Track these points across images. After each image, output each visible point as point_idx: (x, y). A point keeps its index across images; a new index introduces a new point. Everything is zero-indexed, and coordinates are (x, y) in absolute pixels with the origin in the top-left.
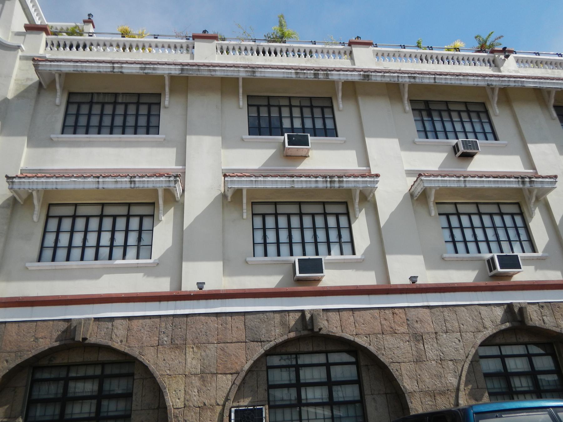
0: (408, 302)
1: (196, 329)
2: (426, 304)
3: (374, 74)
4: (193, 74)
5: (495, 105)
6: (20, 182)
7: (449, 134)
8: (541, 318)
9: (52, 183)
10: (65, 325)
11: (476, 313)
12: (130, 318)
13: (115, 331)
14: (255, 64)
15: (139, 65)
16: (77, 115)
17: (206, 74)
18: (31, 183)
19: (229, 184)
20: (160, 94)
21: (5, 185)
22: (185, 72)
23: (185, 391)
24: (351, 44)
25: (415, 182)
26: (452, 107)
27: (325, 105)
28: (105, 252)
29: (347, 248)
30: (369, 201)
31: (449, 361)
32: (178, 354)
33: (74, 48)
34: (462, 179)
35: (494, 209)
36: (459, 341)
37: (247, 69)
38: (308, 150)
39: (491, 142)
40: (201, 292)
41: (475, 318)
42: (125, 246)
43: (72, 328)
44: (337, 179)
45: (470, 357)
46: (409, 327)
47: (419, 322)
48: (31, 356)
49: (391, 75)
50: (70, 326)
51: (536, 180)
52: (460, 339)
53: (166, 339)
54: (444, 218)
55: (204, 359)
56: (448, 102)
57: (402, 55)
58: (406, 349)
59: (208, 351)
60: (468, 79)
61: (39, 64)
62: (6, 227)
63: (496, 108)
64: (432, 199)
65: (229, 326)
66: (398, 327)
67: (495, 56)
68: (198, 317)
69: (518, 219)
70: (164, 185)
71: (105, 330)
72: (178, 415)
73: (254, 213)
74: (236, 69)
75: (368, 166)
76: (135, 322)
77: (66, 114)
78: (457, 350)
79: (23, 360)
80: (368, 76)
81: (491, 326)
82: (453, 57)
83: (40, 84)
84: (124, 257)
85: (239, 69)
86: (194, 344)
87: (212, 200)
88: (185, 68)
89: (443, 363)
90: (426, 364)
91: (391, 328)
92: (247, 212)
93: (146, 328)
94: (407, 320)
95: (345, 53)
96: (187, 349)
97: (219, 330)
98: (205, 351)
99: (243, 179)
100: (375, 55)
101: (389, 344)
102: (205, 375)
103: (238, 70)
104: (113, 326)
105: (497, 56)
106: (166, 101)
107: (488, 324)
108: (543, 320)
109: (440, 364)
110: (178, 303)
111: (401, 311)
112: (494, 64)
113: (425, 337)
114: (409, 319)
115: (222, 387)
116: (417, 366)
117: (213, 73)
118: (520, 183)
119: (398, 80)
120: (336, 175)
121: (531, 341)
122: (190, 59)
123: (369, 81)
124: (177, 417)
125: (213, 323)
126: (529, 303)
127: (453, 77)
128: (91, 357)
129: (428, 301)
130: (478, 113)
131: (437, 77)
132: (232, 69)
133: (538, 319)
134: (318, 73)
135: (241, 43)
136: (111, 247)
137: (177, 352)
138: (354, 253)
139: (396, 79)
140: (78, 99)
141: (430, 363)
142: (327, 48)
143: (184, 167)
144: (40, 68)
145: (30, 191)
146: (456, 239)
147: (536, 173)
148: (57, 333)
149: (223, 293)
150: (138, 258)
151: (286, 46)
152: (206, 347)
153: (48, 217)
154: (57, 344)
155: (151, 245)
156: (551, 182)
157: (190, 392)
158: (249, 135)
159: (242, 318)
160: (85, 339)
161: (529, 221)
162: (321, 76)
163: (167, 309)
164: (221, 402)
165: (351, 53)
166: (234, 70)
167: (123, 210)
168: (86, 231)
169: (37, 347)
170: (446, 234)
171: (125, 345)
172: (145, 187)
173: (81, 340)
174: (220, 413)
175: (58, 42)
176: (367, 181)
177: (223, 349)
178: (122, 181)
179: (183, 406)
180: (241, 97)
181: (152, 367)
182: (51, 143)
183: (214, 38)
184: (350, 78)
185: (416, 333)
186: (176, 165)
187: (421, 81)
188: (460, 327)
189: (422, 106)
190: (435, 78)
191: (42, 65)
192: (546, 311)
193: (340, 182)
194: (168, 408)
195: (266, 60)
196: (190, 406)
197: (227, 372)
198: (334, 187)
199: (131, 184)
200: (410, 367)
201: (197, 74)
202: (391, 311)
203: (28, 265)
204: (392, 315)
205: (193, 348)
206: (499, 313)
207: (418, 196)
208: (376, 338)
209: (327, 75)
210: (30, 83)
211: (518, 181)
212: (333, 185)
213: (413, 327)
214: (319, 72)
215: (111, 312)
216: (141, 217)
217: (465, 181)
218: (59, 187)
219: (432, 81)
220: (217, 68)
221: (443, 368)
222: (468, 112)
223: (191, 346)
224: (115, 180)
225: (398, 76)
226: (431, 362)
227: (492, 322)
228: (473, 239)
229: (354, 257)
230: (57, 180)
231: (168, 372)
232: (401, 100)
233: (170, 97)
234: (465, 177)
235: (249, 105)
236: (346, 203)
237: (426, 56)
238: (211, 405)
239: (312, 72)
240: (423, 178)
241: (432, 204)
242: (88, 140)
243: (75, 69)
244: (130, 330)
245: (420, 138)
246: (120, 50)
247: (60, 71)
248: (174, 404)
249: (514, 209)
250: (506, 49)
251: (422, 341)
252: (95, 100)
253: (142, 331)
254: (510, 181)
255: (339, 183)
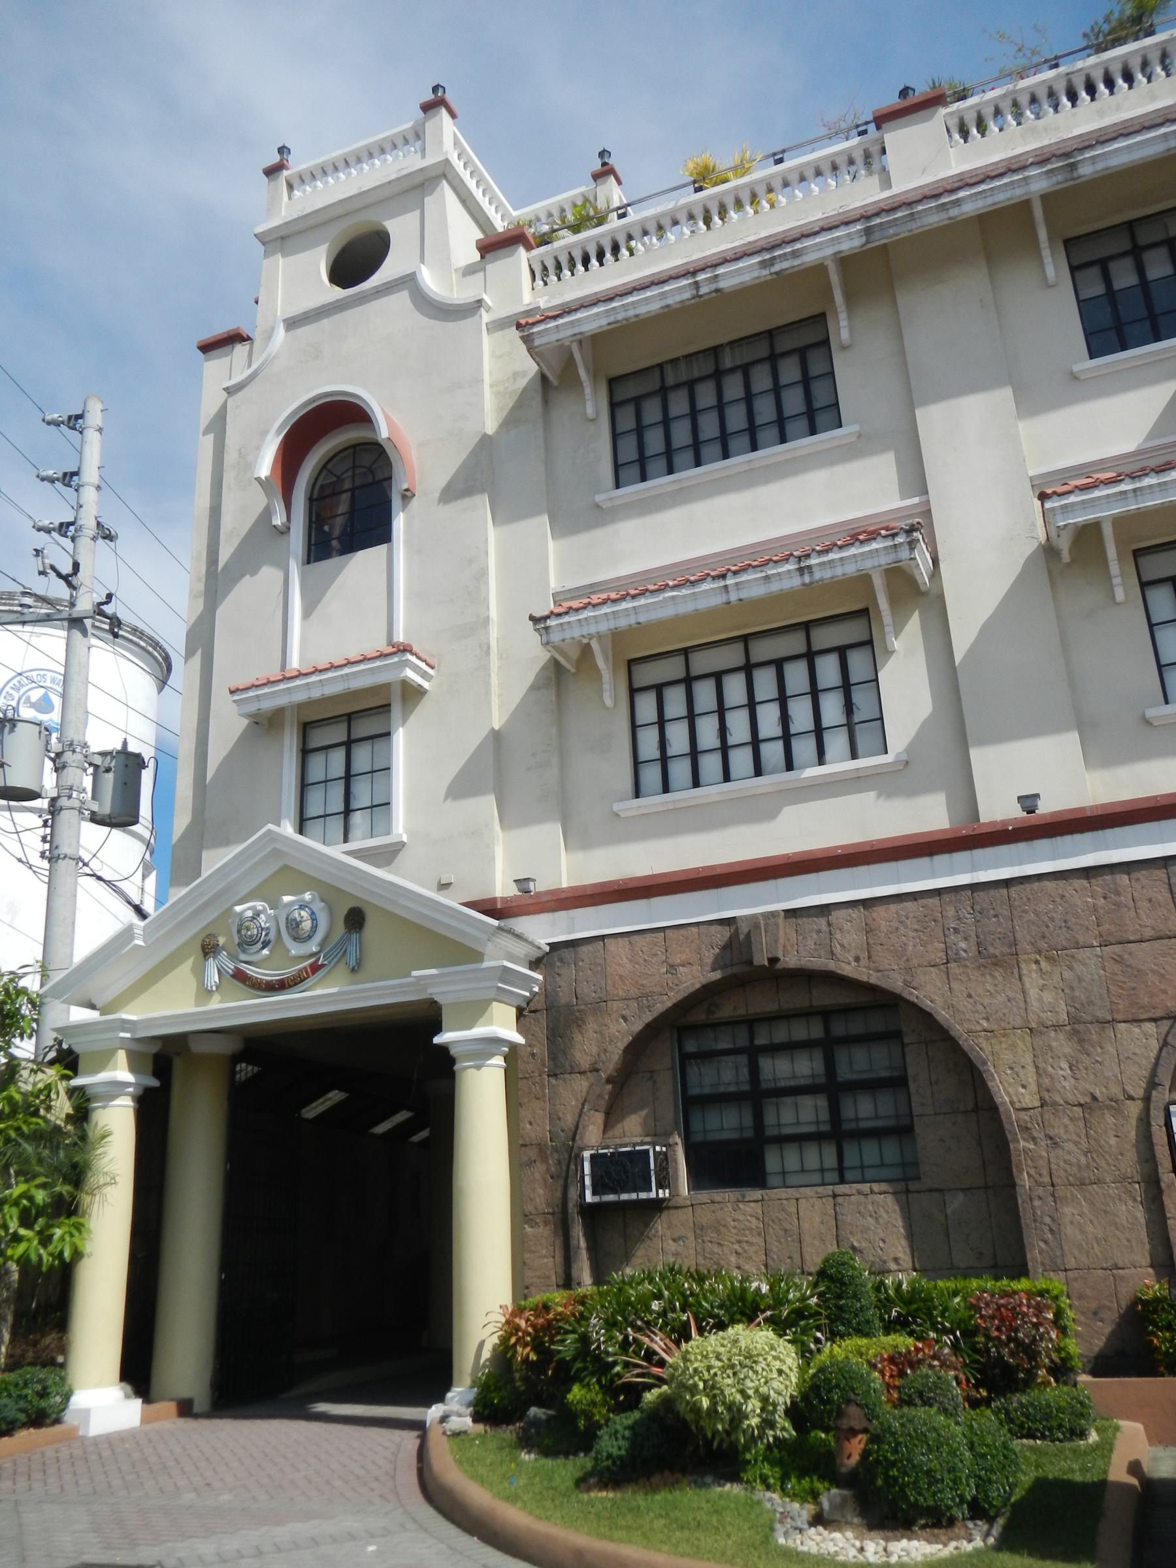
1: (1037, 914)
4: (898, 235)
6: (561, 624)
9: (628, 614)
10: (725, 933)
12: (867, 903)
13: (838, 936)
14: (1070, 136)
15: (756, 256)
16: (639, 431)
17: (934, 220)
18: (584, 623)
19: (1059, 517)
20: (823, 315)
21: (531, 638)
22: (877, 235)
23: (1037, 1067)
28: (773, 752)
32: (1000, 979)
33: (594, 262)
37: (1049, 167)
40: (1033, 819)
42: (819, 731)
43: (742, 937)
48: (669, 1004)
50: (736, 933)
53: (963, 945)
55: (1072, 989)
59: (1079, 968)
61: (532, 334)
62: (554, 731)
65: (1125, 899)
68: (1037, 884)
70: (885, 560)
71: (815, 936)
72: (1029, 1125)
73: (1144, 579)
74: (1016, 178)
76: (880, 912)
77: (615, 436)
79: (655, 1014)
83: (544, 378)
84: (821, 759)
85: (1027, 174)
86: (1039, 952)
87: (1019, 569)
88: (873, 223)
92: (1123, 584)
93: (908, 922)
96: (1023, 965)
97: (1101, 911)
98: (1071, 968)
99: (1097, 493)
102: (1081, 1027)
103: (1025, 179)
104: (829, 925)
106: (842, 329)
110: (979, 854)
115: (1135, 1054)
117: (954, 212)
122: (883, 189)
124: (1027, 1129)
125: (1079, 894)
128: (795, 999)
132: (1005, 180)
135: (1015, 86)
136: (787, 737)
137: (997, 974)
140: (631, 390)
143: (924, 498)
144: (537, 342)
145: (585, 641)
148: (712, 951)
149: (1095, 814)
150: (854, 756)
152: (1073, 957)
153: (633, 692)
154: (717, 975)
155: (881, 719)
157: (1050, 1069)
158: (1091, 358)
159: (1161, 874)
160: (774, 960)
163: (952, 873)
164: (1139, 1092)
166: (1012, 183)
167: (794, 643)
168: (721, 711)
169: (677, 985)
171: (869, 968)
172: (837, 576)
173: (766, 963)
174: (1140, 1119)
175: (556, 258)
177: (1119, 960)
178: (779, 574)
179: (1037, 1103)
180: (1046, 253)
181: (943, 1015)
182: (600, 516)
183: (935, 100)
186: (902, 499)
191: (539, 332)
194: (1001, 1109)
195: (1101, 113)
196: (1055, 1104)
197: (1142, 1017)
199: (802, 575)
201: (910, 231)
203: (617, 807)
205: (1037, 962)
210: (523, 382)
215: (820, 892)
216: (842, 652)
218: (643, 618)
220: (962, 194)
223: (1033, 956)
224: (763, 574)
230: (636, 604)
231: (985, 1024)
233: (849, 318)
235: (1073, 269)
238: (1111, 1100)
242: (676, 487)
243: (612, 319)
244: (871, 931)
246: (699, 229)
247: (581, 333)
248: (1015, 1099)
252: (670, 380)
253: (902, 930)
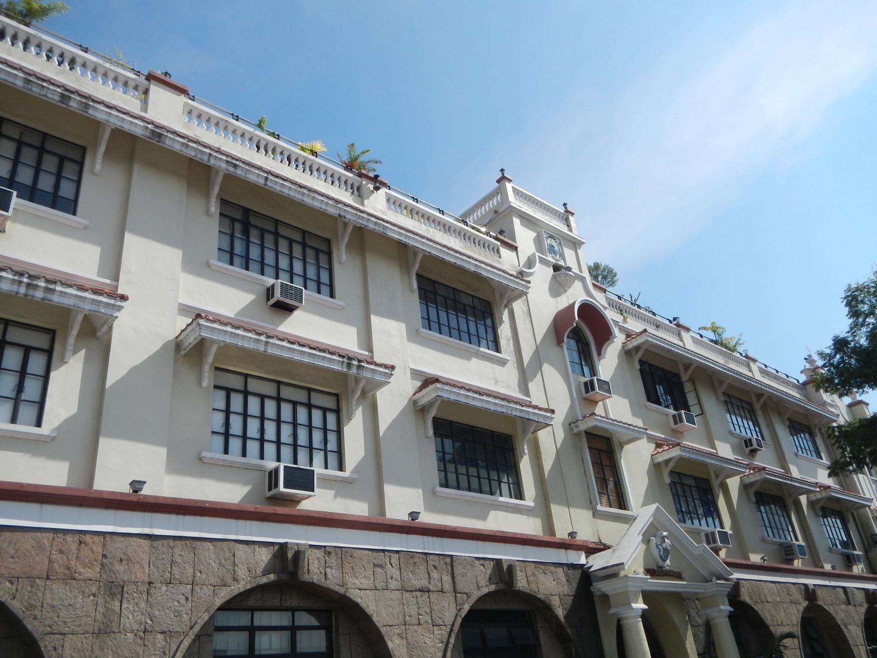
0: (115, 525)
2: (146, 531)
3: (171, 136)
5: (344, 248)
7: (266, 269)
8: (323, 571)
11: (228, 555)
24: (150, 77)
25: (188, 325)
26: (282, 231)
27: (69, 156)
29: (27, 412)
30: (98, 339)
31: (160, 633)
34: (263, 338)
35: (301, 397)
36: (187, 599)
38: (6, 218)
39: (325, 298)
41: (224, 563)
44: (42, 284)
45: (197, 629)
46: (104, 570)
47: (124, 562)
49: (200, 148)
51: (366, 366)
52: (190, 597)
54: (222, 394)
56: (279, 223)
57: (230, 129)
58: (84, 609)
60: (314, 198)
63: (344, 252)
64: (210, 359)
66: (83, 568)
67: (362, 182)
69: (331, 419)
75: (116, 279)
78: (178, 614)
80: (160, 135)
81: (245, 578)
82: (305, 161)
89: (146, 637)
90: (115, 639)
91: (68, 568)
94: (104, 556)
95: (136, 88)
100: (186, 112)
101: (53, 599)
105: (364, 182)
107: (242, 573)
108: (325, 574)
109: (141, 638)
111: (96, 538)
112: (358, 192)
113: (128, 589)
114: (108, 555)
116: (98, 641)
118: (345, 365)
119: (209, 160)
120: (44, 277)
121: (301, 605)
123: (160, 144)
126: (311, 546)
127: (293, 187)
129: (151, 527)
130: (317, 251)
131: (271, 177)
133: (318, 572)
134: (70, 97)
138: (39, 424)
139: (206, 158)
141: (123, 637)
142: (106, 68)
146: (231, 432)
147: (372, 357)
151: (26, 32)
156: (385, 373)
161: (345, 424)
162: (73, 104)
165: (146, 92)
170: (218, 420)
176: (100, 302)
184: (126, 127)
185: (114, 580)
187: (244, 175)
188: (194, 576)
189: (238, 215)
190: (266, 178)
192: (333, 561)
193: (47, 290)
198: (33, 297)
200: (82, 643)
202: (76, 538)
204: (76, 545)
206: (264, 556)
207: (188, 349)
208: (31, 586)
209: (87, 106)
211: (343, 362)
212: (31, 292)
213: (110, 570)
214: (72, 96)
217: (267, 343)
219: (262, 181)
221: (144, 645)
222: (304, 245)
225: (210, 154)
226: (125, 635)
227: (249, 571)
228: (257, 436)
229: (36, 430)
232: (207, 194)
234: (268, 337)
236: (52, 333)
237: (267, 144)
239: (59, 90)
240: (202, 322)
241: (207, 368)
245: (219, 260)
249: (329, 403)
250: (379, 179)
251: (119, 597)
254: (332, 359)
255: (44, 292)
